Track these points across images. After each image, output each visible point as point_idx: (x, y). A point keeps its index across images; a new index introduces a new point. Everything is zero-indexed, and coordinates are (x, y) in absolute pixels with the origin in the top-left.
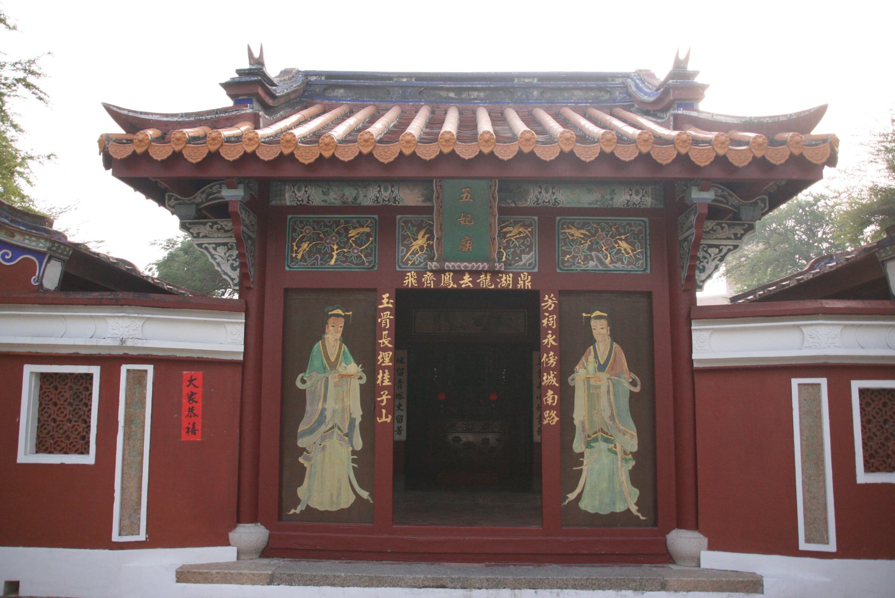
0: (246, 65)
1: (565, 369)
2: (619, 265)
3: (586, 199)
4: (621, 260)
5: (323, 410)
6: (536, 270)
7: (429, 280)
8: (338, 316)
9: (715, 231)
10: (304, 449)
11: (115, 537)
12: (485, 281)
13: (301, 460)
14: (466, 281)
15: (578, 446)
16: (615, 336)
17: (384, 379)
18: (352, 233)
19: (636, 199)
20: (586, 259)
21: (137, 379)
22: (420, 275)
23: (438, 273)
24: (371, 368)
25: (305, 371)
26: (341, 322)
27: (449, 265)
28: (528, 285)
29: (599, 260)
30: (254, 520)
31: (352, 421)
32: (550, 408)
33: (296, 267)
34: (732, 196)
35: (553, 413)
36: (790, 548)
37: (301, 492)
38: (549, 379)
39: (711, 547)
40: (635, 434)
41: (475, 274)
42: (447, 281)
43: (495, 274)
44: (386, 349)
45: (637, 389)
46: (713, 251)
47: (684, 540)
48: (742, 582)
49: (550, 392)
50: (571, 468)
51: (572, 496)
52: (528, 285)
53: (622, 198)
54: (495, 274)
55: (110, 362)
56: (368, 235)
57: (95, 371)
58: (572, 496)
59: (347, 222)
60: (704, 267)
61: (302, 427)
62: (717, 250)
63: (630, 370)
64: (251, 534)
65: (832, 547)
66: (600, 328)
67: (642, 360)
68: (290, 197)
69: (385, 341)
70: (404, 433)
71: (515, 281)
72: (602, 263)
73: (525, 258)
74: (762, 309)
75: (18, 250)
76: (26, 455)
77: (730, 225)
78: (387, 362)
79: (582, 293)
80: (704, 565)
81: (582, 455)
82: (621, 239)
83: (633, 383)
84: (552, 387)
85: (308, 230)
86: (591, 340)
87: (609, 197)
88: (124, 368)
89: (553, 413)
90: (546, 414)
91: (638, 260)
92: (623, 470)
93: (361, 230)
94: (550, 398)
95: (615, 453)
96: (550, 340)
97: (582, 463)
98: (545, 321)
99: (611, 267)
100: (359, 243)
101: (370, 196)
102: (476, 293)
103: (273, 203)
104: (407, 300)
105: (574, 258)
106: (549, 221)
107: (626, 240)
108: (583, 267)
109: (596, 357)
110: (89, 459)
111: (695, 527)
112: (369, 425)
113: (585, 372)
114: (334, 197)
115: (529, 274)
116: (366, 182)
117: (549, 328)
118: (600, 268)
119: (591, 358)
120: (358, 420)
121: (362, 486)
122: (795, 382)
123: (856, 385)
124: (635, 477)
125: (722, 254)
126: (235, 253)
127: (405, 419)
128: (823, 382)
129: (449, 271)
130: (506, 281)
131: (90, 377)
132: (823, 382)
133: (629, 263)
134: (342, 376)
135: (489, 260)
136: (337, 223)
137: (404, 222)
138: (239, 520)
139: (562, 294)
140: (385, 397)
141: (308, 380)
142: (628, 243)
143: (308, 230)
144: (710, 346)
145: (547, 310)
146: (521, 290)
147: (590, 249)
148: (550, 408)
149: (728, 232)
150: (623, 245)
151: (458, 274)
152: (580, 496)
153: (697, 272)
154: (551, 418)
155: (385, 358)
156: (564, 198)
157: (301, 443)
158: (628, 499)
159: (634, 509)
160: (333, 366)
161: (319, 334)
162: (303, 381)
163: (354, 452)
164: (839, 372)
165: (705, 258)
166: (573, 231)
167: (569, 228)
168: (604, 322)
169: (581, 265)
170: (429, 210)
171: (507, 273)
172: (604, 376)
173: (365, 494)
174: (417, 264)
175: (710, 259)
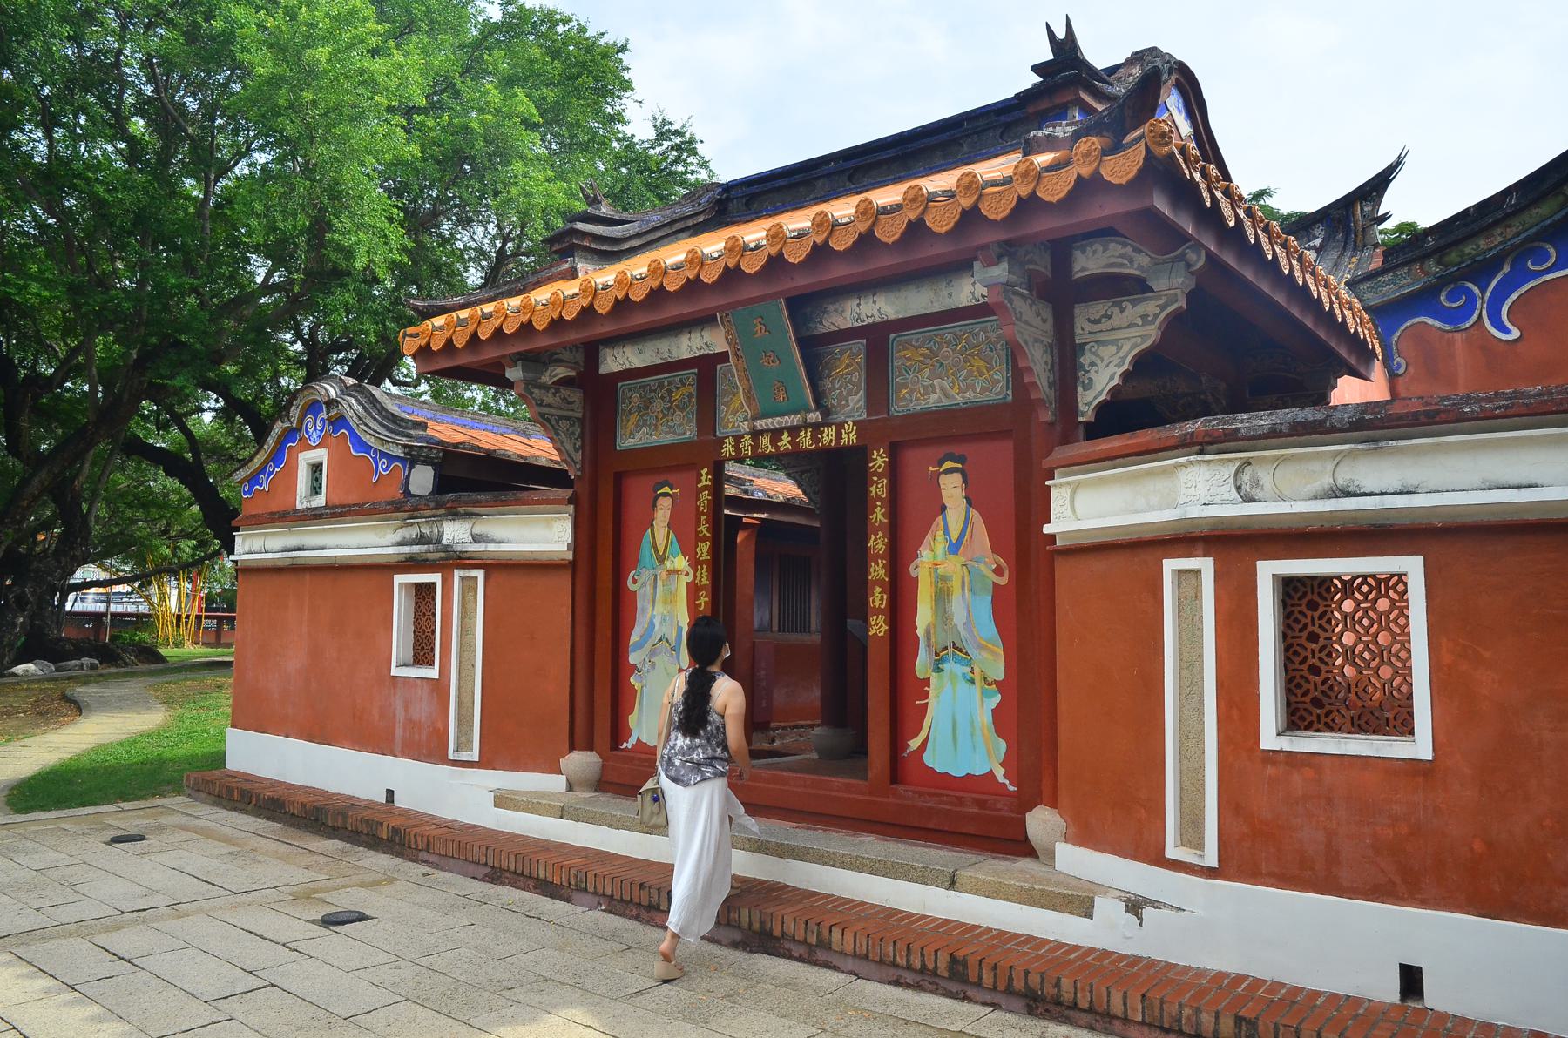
4: (971, 387)
5: (653, 616)
9: (1110, 317)
10: (635, 667)
11: (451, 757)
12: (805, 439)
14: (785, 442)
15: (922, 665)
18: (676, 396)
21: (469, 583)
28: (854, 438)
29: (943, 390)
30: (589, 747)
31: (680, 629)
32: (878, 611)
34: (1139, 251)
40: (1000, 651)
41: (794, 431)
45: (1003, 581)
46: (1107, 351)
48: (1065, 896)
49: (879, 589)
51: (914, 744)
53: (967, 291)
54: (816, 428)
59: (670, 383)
60: (1091, 380)
61: (635, 637)
62: (1114, 349)
63: (995, 550)
64: (581, 761)
65: (1211, 860)
68: (614, 361)
71: (838, 436)
72: (946, 396)
73: (853, 400)
74: (1103, 447)
80: (1060, 864)
81: (927, 682)
82: (972, 355)
83: (998, 571)
84: (879, 582)
86: (944, 508)
87: (946, 293)
90: (873, 620)
94: (878, 599)
95: (972, 681)
97: (926, 695)
98: (873, 489)
99: (959, 399)
103: (603, 370)
105: (911, 392)
108: (923, 405)
109: (946, 532)
111: (1053, 804)
115: (855, 423)
117: (878, 497)
118: (946, 402)
122: (1170, 565)
125: (1121, 354)
128: (1205, 565)
130: (828, 436)
133: (984, 390)
134: (670, 572)
138: (572, 748)
141: (639, 582)
144: (1085, 505)
145: (876, 473)
146: (844, 447)
148: (878, 611)
149: (1132, 312)
150: (979, 363)
153: (1080, 389)
154: (878, 626)
157: (633, 659)
160: (662, 560)
162: (635, 581)
164: (1234, 544)
165: (1093, 364)
167: (905, 349)
169: (917, 405)
171: (829, 425)
175: (1101, 365)
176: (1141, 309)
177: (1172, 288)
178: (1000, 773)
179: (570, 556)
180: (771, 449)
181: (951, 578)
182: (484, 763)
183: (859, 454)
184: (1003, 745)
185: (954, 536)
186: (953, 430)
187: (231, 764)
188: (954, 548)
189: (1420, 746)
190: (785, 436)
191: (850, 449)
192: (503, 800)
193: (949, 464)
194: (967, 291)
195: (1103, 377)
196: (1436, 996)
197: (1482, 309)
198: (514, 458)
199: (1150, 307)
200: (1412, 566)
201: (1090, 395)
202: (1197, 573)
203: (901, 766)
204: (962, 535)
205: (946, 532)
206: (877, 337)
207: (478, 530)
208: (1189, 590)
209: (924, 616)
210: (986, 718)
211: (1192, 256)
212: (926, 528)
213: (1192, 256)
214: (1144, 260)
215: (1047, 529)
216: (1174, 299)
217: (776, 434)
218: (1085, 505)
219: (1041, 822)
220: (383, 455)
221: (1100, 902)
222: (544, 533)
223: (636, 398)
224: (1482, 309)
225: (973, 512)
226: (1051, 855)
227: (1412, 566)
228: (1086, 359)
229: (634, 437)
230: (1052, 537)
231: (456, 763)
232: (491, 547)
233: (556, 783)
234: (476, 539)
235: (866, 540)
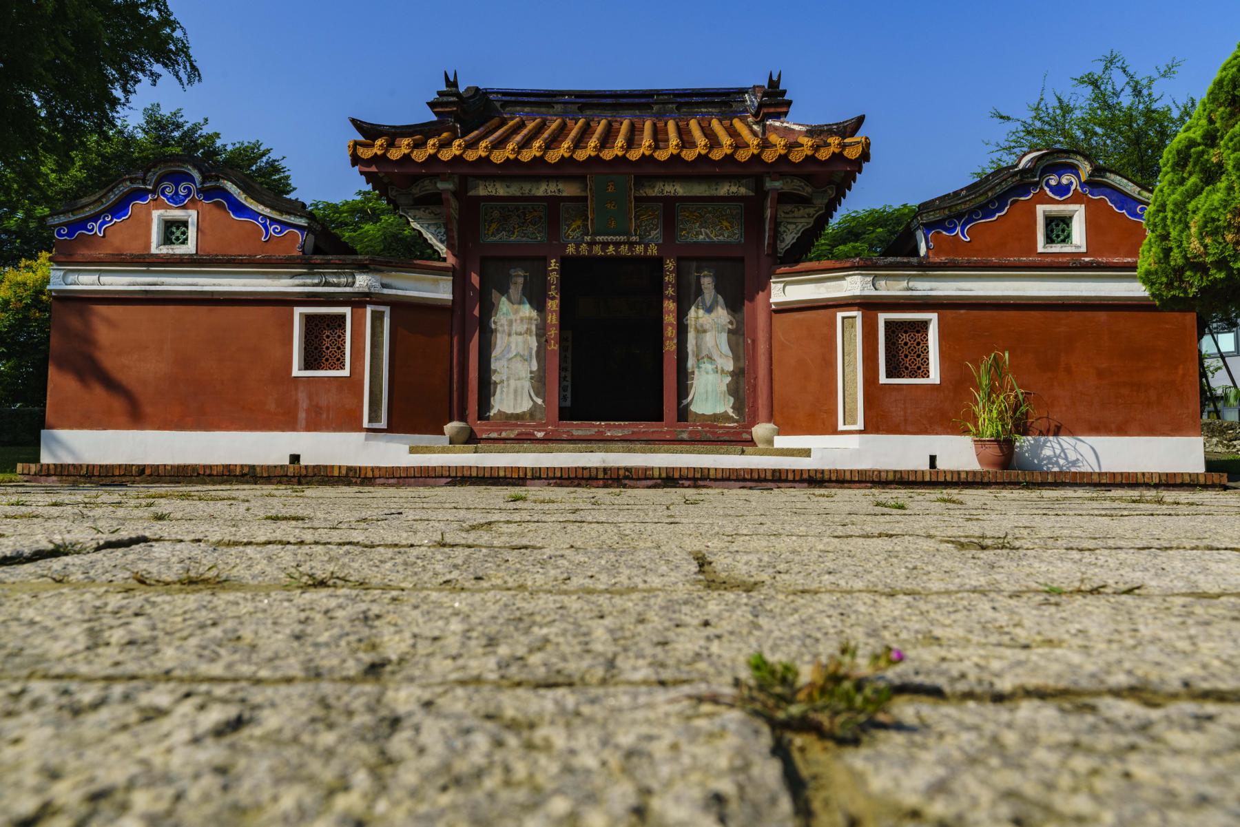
1: (682, 314)
2: (721, 238)
12: (624, 250)
16: (718, 289)
17: (553, 319)
19: (734, 189)
20: (698, 234)
22: (578, 246)
23: (591, 244)
26: (521, 280)
27: (599, 238)
28: (655, 252)
36: (835, 431)
41: (617, 244)
42: (597, 250)
43: (632, 245)
44: (553, 298)
46: (791, 227)
53: (724, 190)
54: (632, 245)
65: (860, 425)
66: (707, 283)
70: (569, 400)
71: (646, 250)
73: (653, 233)
76: (296, 372)
81: (693, 373)
83: (731, 323)
84: (671, 324)
86: (699, 292)
96: (670, 291)
101: (542, 190)
102: (618, 260)
103: (471, 193)
106: (670, 209)
110: (346, 372)
112: (541, 354)
113: (695, 315)
114: (514, 190)
116: (538, 179)
117: (669, 283)
120: (535, 349)
121: (537, 395)
122: (840, 315)
124: (734, 390)
126: (443, 230)
127: (569, 389)
128: (857, 314)
129: (599, 243)
130: (639, 250)
136: (517, 209)
139: (679, 260)
140: (553, 332)
150: (725, 223)
154: (670, 346)
158: (725, 406)
159: (730, 412)
163: (531, 372)
164: (869, 306)
169: (692, 239)
170: (586, 198)
173: (539, 401)
176: (807, 210)
183: (658, 262)
184: (732, 400)
185: (708, 303)
190: (611, 248)
191: (651, 258)
194: (724, 190)
197: (959, 229)
199: (812, 211)
200: (933, 317)
201: (783, 245)
203: (683, 414)
206: (670, 202)
207: (385, 281)
210: (725, 388)
214: (809, 189)
216: (820, 209)
217: (605, 245)
220: (274, 221)
223: (496, 214)
224: (959, 229)
228: (782, 229)
231: (368, 430)
232: (400, 292)
233: (443, 440)
234: (384, 286)
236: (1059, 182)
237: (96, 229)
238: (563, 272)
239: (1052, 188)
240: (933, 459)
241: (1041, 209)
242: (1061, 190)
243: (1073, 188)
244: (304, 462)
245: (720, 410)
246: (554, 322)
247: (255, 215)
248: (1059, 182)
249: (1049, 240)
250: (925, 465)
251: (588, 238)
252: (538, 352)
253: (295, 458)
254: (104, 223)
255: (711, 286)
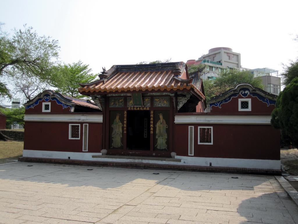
0: (102, 71)
1: (155, 124)
2: (164, 105)
3: (158, 94)
4: (165, 105)
5: (116, 131)
6: (150, 107)
7: (132, 109)
8: (118, 115)
11: (83, 151)
12: (141, 109)
13: (113, 139)
14: (138, 109)
15: (157, 137)
16: (164, 118)
17: (125, 126)
21: (86, 126)
22: (131, 108)
24: (123, 124)
25: (113, 124)
26: (119, 116)
27: (135, 106)
28: (149, 109)
30: (105, 149)
31: (121, 132)
32: (152, 131)
33: (112, 107)
35: (152, 131)
36: (187, 155)
37: (112, 144)
38: (152, 126)
39: (177, 155)
41: (140, 108)
42: (135, 109)
43: (143, 108)
45: (167, 128)
47: (173, 154)
50: (155, 141)
51: (156, 146)
52: (149, 109)
55: (82, 123)
56: (123, 101)
57: (80, 125)
58: (156, 146)
61: (113, 134)
62: (182, 102)
64: (104, 151)
66: (161, 117)
67: (167, 123)
69: (125, 119)
73: (148, 104)
75: (67, 106)
76: (70, 138)
77: (184, 98)
78: (126, 123)
79: (158, 111)
80: (175, 158)
81: (158, 139)
83: (167, 126)
85: (113, 100)
86: (160, 119)
88: (84, 124)
89: (152, 131)
91: (167, 104)
92: (164, 141)
93: (121, 100)
94: (152, 129)
96: (152, 119)
100: (121, 102)
101: (122, 95)
102: (140, 111)
104: (129, 112)
106: (152, 98)
107: (166, 101)
109: (160, 122)
110: (79, 139)
111: (174, 152)
112: (123, 133)
113: (158, 124)
117: (152, 117)
119: (159, 122)
120: (121, 132)
122: (189, 127)
123: (199, 127)
128: (193, 127)
130: (145, 109)
131: (79, 126)
132: (193, 127)
134: (119, 125)
135: (142, 105)
137: (129, 99)
138: (102, 149)
139: (154, 111)
140: (125, 129)
141: (114, 126)
142: (166, 102)
143: (113, 100)
144: (179, 119)
147: (159, 103)
148: (152, 131)
149: (184, 99)
150: (165, 102)
151: (137, 108)
152: (157, 146)
154: (152, 132)
155: (125, 122)
156: (154, 94)
157: (113, 136)
159: (166, 148)
161: (115, 118)
163: (121, 138)
164: (196, 125)
166: (156, 100)
168: (162, 116)
172: (161, 125)
173: (122, 145)
174: (131, 105)
177: (188, 97)
178: (166, 148)
179: (102, 122)
180: (136, 110)
181: (161, 126)
182: (88, 152)
185: (161, 122)
186: (162, 110)
187: (23, 156)
188: (161, 124)
189: (212, 144)
190: (138, 108)
191: (148, 111)
192: (93, 157)
193: (161, 114)
195: (180, 106)
196: (212, 165)
198: (85, 106)
199: (186, 99)
200: (212, 127)
201: (179, 107)
202: (192, 127)
203: (155, 149)
204: (162, 122)
205: (160, 122)
208: (191, 129)
209: (157, 132)
211: (191, 94)
212: (158, 121)
213: (191, 94)
215: (174, 122)
216: (188, 98)
217: (137, 108)
218: (179, 119)
219: (173, 154)
220: (65, 105)
221: (182, 160)
222: (98, 119)
225: (164, 120)
226: (174, 157)
227: (212, 127)
228: (179, 103)
229: (112, 105)
230: (175, 123)
233: (100, 154)
235: (150, 122)
236: (245, 93)
237: (32, 107)
238: (127, 114)
239: (243, 95)
240: (211, 164)
241: (240, 100)
242: (245, 95)
243: (248, 94)
244: (71, 158)
245: (164, 148)
246: (125, 126)
247: (62, 103)
248: (245, 93)
249: (242, 107)
250: (209, 165)
251: (133, 106)
252: (122, 133)
253: (69, 158)
254: (34, 105)
255: (162, 117)
